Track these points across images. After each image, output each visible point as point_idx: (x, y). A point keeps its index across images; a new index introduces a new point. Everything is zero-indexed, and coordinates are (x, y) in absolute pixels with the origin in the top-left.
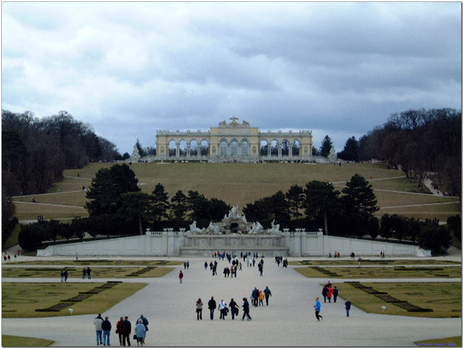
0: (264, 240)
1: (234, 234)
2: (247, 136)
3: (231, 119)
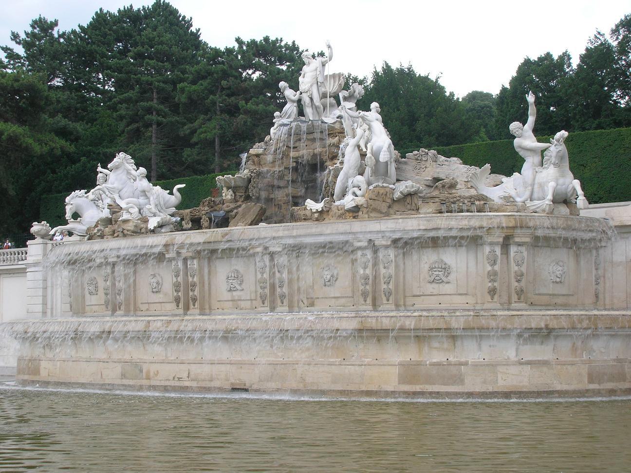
0: (429, 258)
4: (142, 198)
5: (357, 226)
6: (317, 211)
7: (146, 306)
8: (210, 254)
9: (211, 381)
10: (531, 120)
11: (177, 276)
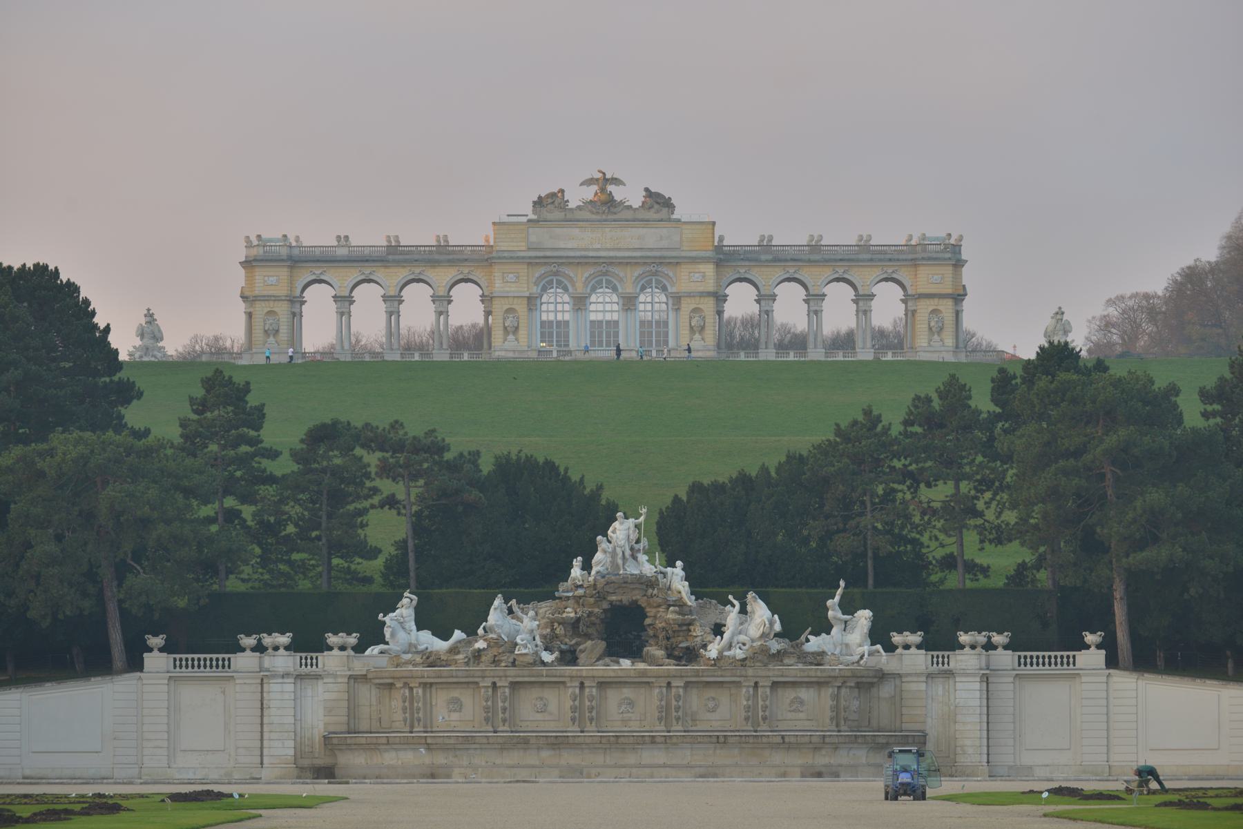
0: (788, 695)
1: (626, 663)
2: (662, 261)
3: (590, 182)
5: (750, 672)
10: (837, 598)
11: (574, 700)
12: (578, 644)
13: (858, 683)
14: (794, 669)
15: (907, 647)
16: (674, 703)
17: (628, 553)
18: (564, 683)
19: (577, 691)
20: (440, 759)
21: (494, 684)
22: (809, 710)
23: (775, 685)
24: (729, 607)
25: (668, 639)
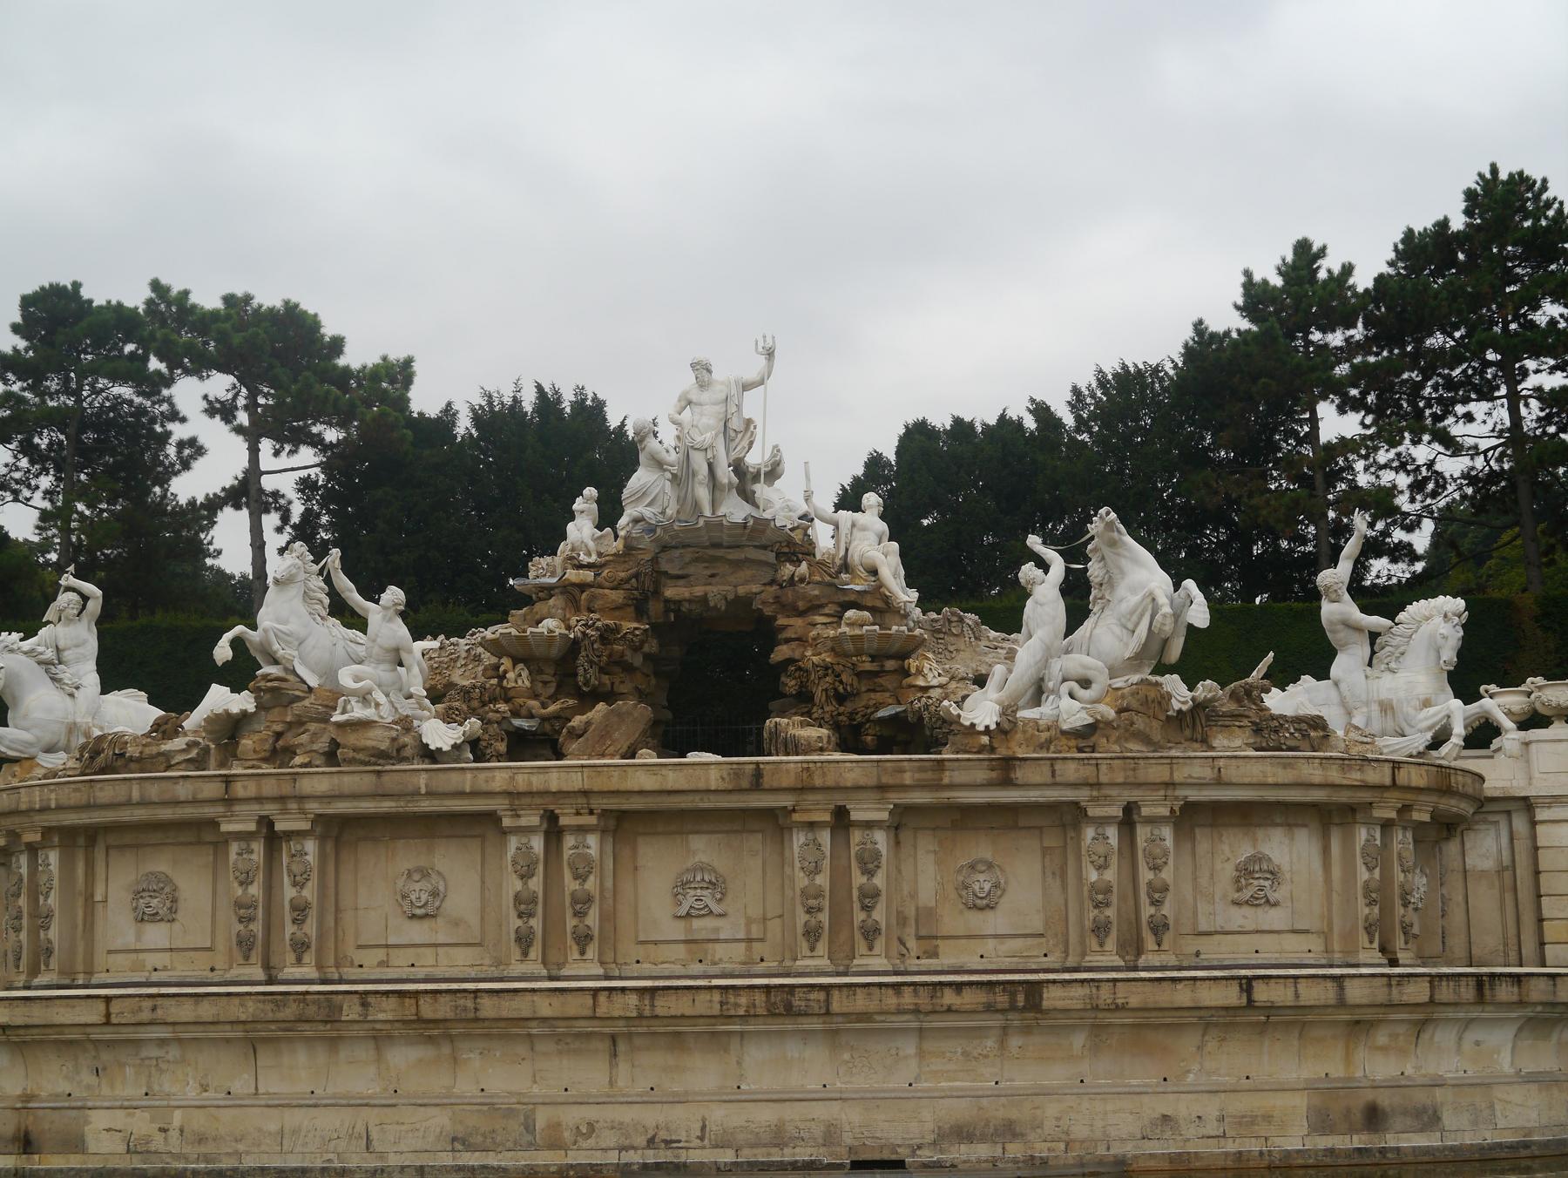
0: (1235, 848)
4: (382, 667)
6: (987, 730)
7: (380, 954)
8: (627, 822)
9: (781, 1145)
11: (525, 876)
12: (563, 718)
13: (1434, 815)
14: (1236, 762)
15: (1533, 720)
16: (859, 879)
17: (726, 474)
18: (492, 818)
19: (537, 843)
20: (54, 1079)
21: (266, 823)
22: (1283, 906)
23: (1194, 817)
24: (1028, 571)
25: (841, 699)
